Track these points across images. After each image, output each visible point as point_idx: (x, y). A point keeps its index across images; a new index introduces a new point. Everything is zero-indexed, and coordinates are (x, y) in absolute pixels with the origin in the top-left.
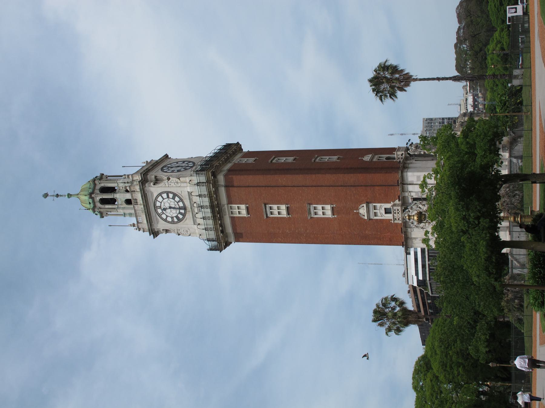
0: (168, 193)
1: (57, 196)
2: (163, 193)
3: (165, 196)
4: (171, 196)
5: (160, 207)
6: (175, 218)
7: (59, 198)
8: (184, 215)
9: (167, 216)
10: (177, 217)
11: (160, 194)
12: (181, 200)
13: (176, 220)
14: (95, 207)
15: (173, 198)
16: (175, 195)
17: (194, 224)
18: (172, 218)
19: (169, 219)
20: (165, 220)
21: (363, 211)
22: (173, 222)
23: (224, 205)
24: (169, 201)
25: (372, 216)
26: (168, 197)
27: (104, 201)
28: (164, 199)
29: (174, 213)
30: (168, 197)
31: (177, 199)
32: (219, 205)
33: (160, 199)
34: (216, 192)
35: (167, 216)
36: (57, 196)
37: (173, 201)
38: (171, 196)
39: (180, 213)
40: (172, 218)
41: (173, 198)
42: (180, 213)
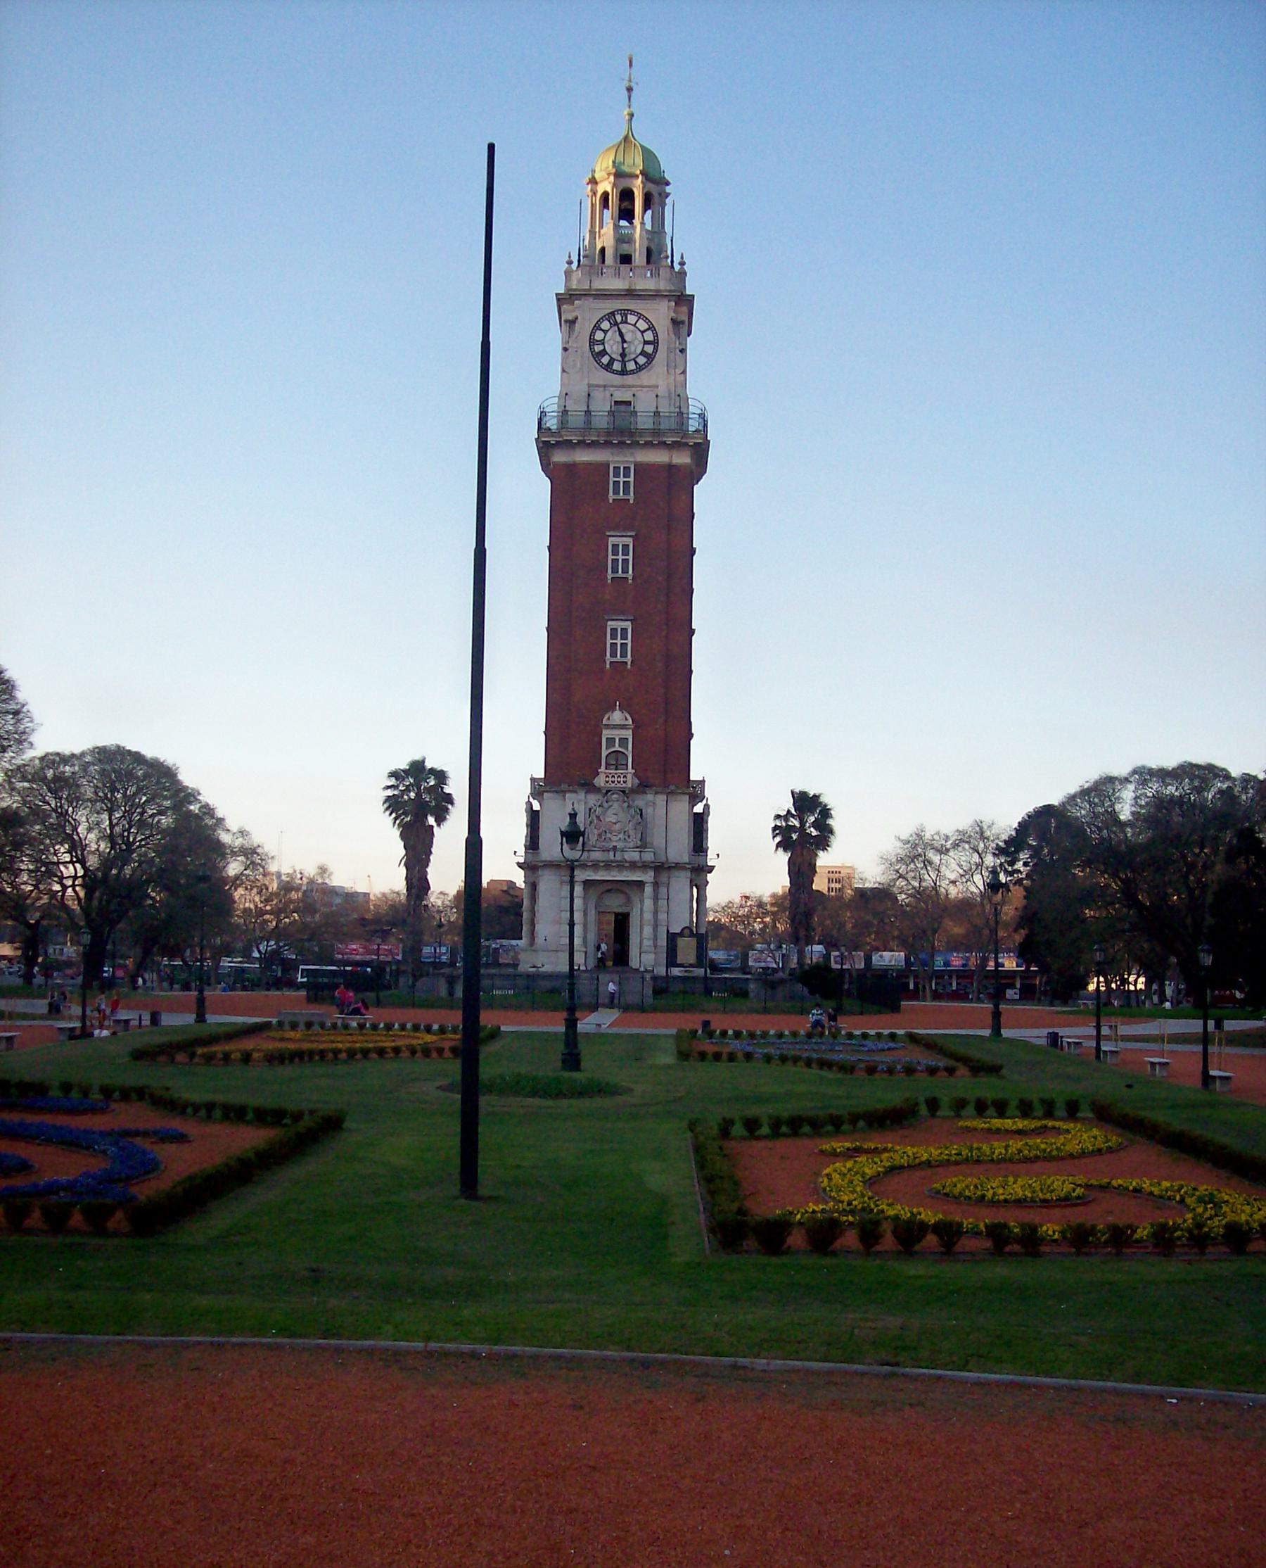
0: (655, 343)
1: (630, 90)
2: (656, 335)
3: (649, 336)
4: (649, 349)
6: (601, 347)
7: (626, 93)
8: (608, 367)
9: (605, 332)
10: (604, 353)
11: (651, 328)
12: (640, 368)
13: (598, 348)
15: (643, 353)
16: (650, 357)
17: (589, 386)
18: (602, 342)
19: (599, 335)
20: (597, 327)
21: (617, 716)
22: (592, 342)
23: (632, 454)
24: (636, 342)
25: (606, 733)
26: (646, 343)
27: (627, 195)
28: (643, 332)
29: (613, 347)
30: (646, 343)
31: (642, 360)
33: (642, 325)
35: (605, 332)
36: (630, 90)
37: (639, 351)
38: (649, 349)
39: (612, 361)
40: (602, 342)
41: (643, 353)
42: (612, 361)
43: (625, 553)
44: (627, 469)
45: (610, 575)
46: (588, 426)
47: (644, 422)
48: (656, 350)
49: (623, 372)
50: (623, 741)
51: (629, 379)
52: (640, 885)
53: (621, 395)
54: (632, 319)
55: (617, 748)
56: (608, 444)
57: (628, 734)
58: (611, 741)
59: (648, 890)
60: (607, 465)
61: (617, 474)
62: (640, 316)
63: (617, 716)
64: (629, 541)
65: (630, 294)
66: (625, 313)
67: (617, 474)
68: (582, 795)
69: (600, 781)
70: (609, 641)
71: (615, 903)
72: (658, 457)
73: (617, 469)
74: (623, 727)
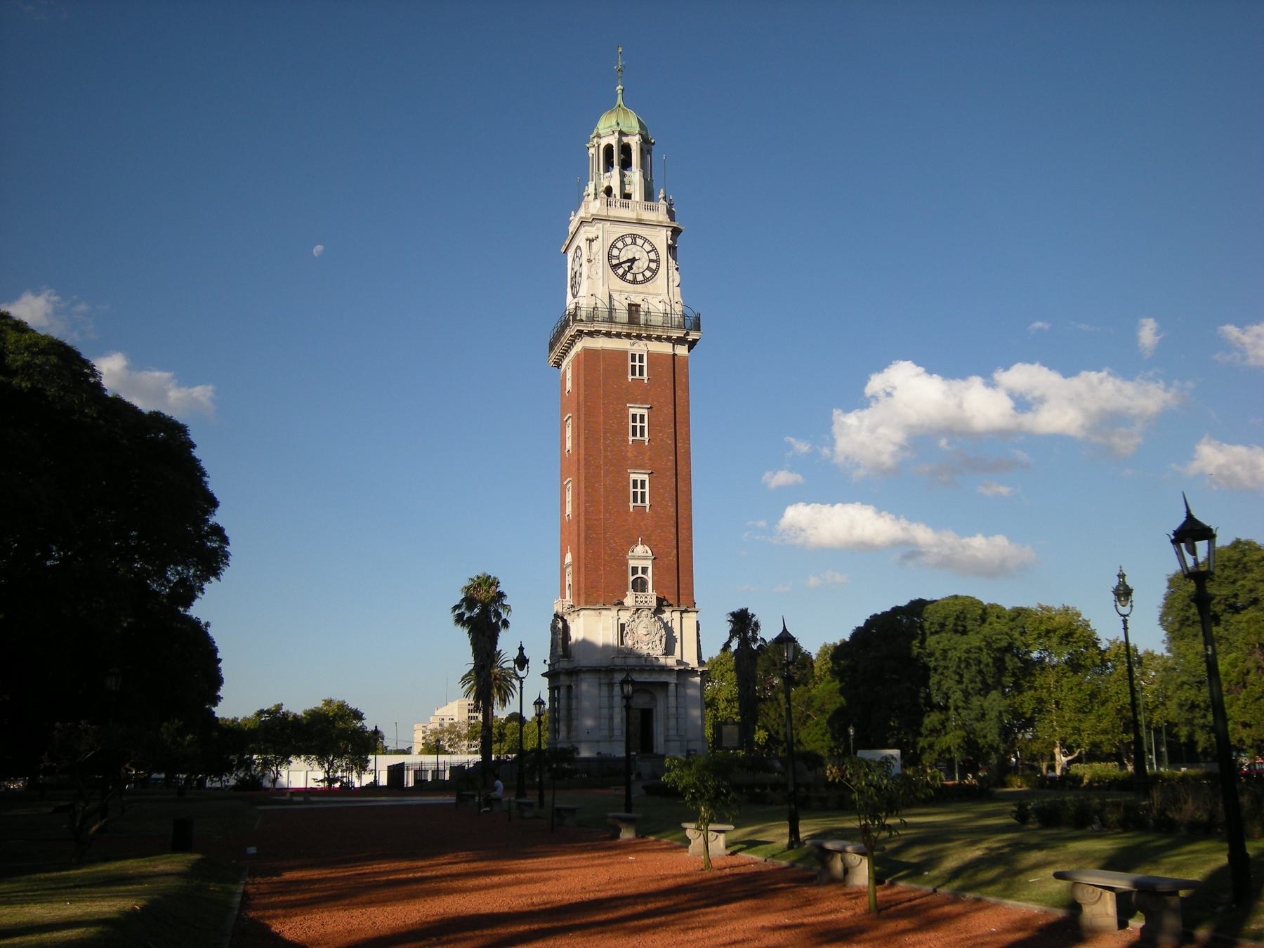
0: (657, 261)
4: (653, 265)
5: (634, 243)
9: (620, 250)
11: (654, 250)
12: (646, 280)
13: (615, 262)
14: (622, 134)
15: (648, 268)
16: (655, 272)
20: (613, 246)
21: (640, 549)
22: (610, 257)
25: (632, 563)
27: (626, 149)
30: (651, 261)
31: (648, 274)
32: (649, 338)
34: (669, 339)
38: (653, 265)
41: (648, 268)
43: (642, 420)
44: (641, 357)
45: (631, 438)
46: (611, 319)
47: (657, 319)
48: (658, 266)
49: (634, 282)
50: (644, 570)
51: (639, 288)
52: (666, 684)
53: (636, 300)
54: (640, 242)
55: (640, 574)
56: (628, 336)
57: (649, 564)
58: (635, 570)
59: (672, 688)
60: (626, 352)
61: (633, 360)
62: (646, 240)
63: (640, 549)
64: (645, 412)
65: (640, 222)
66: (634, 237)
67: (633, 360)
68: (614, 612)
69: (629, 600)
70: (632, 490)
71: (641, 701)
72: (665, 348)
73: (633, 356)
74: (645, 558)
